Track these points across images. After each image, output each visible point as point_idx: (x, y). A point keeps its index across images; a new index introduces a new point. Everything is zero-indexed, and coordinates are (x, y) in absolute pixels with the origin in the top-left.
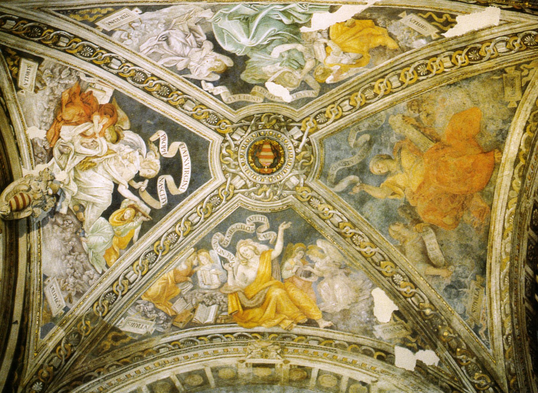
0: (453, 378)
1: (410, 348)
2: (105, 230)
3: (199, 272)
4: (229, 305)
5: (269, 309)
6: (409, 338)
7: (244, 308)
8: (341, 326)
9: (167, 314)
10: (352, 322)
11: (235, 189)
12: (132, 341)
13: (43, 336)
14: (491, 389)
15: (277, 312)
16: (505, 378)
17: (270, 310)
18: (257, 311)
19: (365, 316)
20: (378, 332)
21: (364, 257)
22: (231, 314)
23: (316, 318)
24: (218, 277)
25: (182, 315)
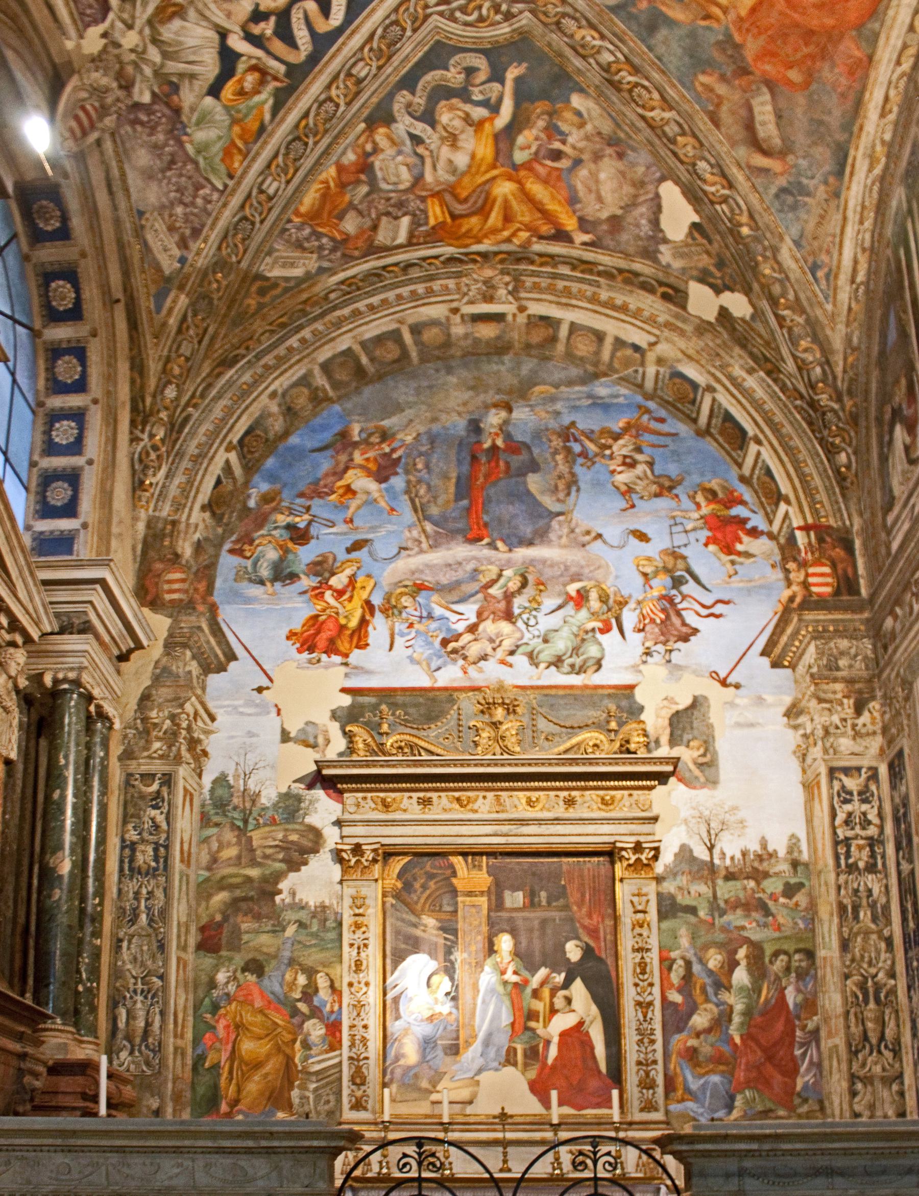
0: (767, 344)
1: (712, 286)
2: (218, 117)
3: (377, 162)
4: (431, 214)
5: (493, 215)
6: (712, 269)
7: (454, 217)
8: (608, 241)
9: (333, 239)
10: (624, 237)
11: (426, 6)
12: (286, 290)
13: (159, 309)
14: (818, 370)
15: (508, 218)
16: (841, 356)
17: (495, 218)
18: (474, 220)
19: (645, 228)
20: (666, 255)
21: (652, 128)
22: (433, 228)
23: (569, 228)
24: (409, 170)
25: (357, 237)
